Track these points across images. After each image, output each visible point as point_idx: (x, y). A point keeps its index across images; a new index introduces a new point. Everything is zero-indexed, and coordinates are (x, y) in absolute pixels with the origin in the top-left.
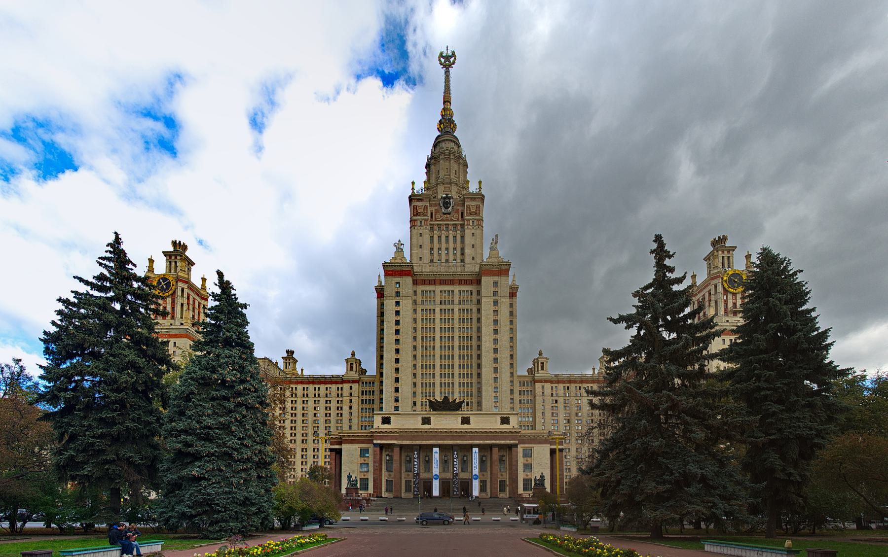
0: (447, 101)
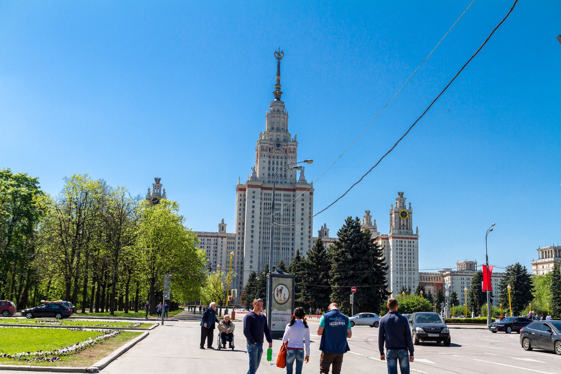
0: (279, 81)
